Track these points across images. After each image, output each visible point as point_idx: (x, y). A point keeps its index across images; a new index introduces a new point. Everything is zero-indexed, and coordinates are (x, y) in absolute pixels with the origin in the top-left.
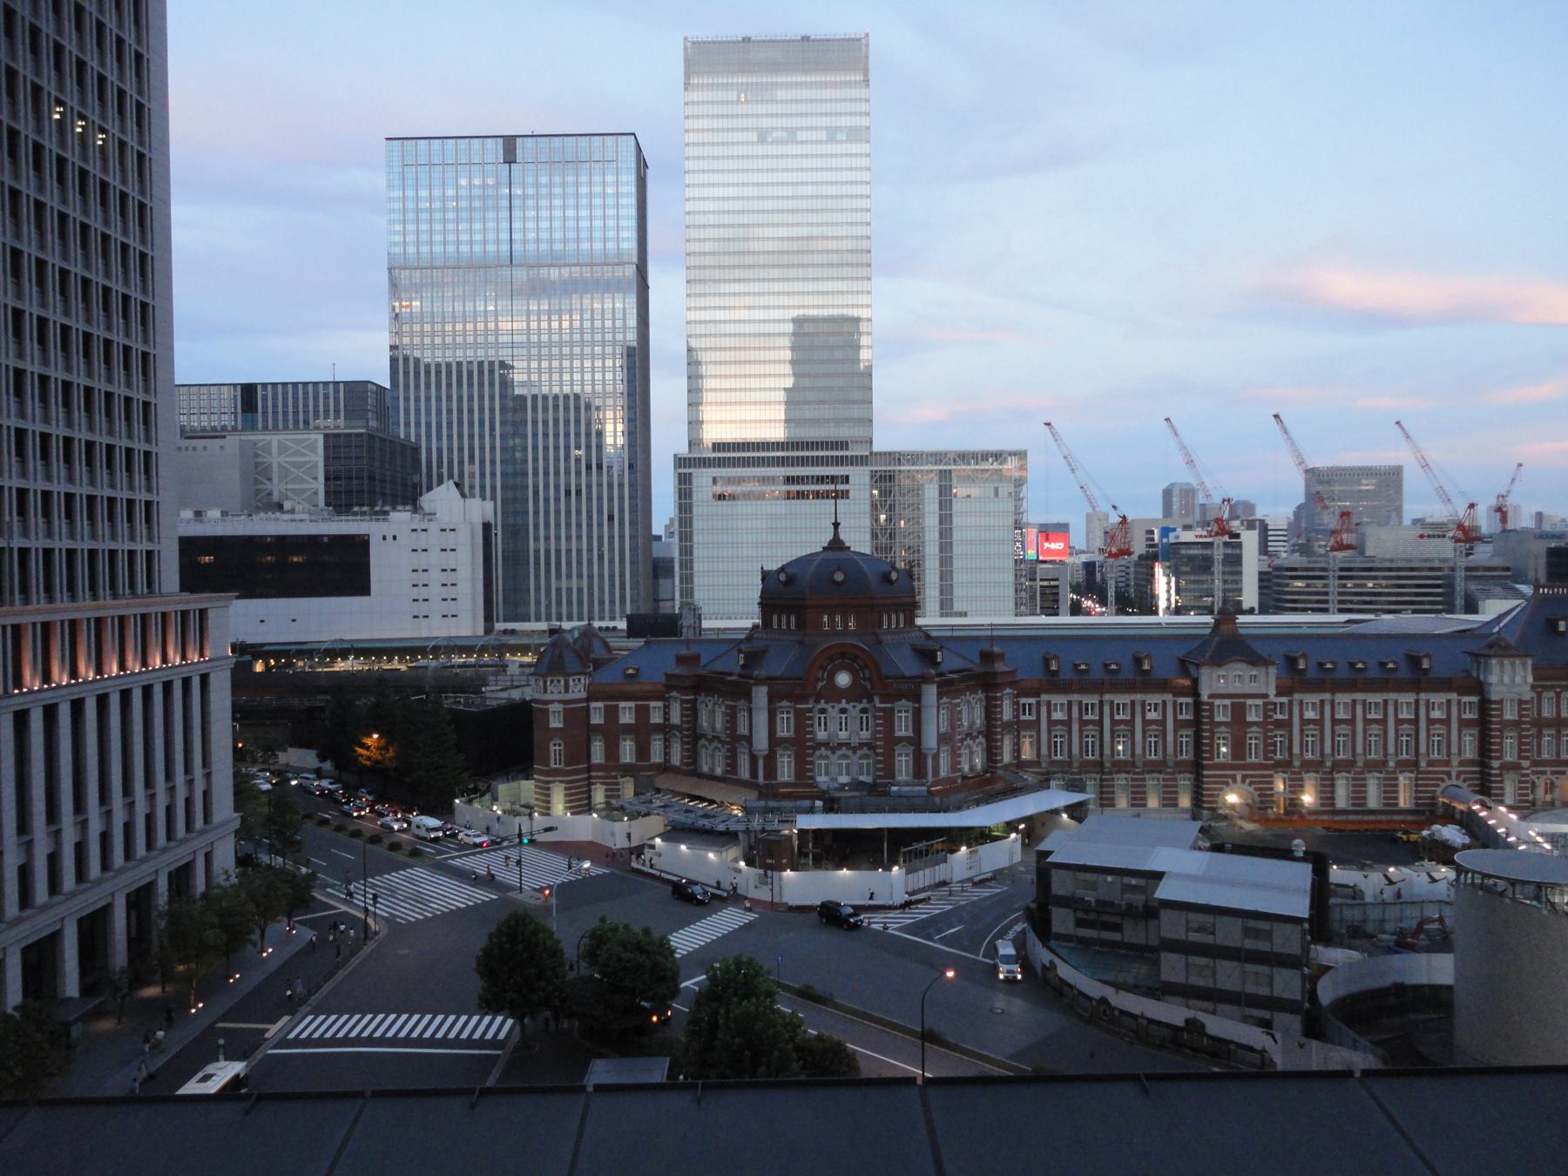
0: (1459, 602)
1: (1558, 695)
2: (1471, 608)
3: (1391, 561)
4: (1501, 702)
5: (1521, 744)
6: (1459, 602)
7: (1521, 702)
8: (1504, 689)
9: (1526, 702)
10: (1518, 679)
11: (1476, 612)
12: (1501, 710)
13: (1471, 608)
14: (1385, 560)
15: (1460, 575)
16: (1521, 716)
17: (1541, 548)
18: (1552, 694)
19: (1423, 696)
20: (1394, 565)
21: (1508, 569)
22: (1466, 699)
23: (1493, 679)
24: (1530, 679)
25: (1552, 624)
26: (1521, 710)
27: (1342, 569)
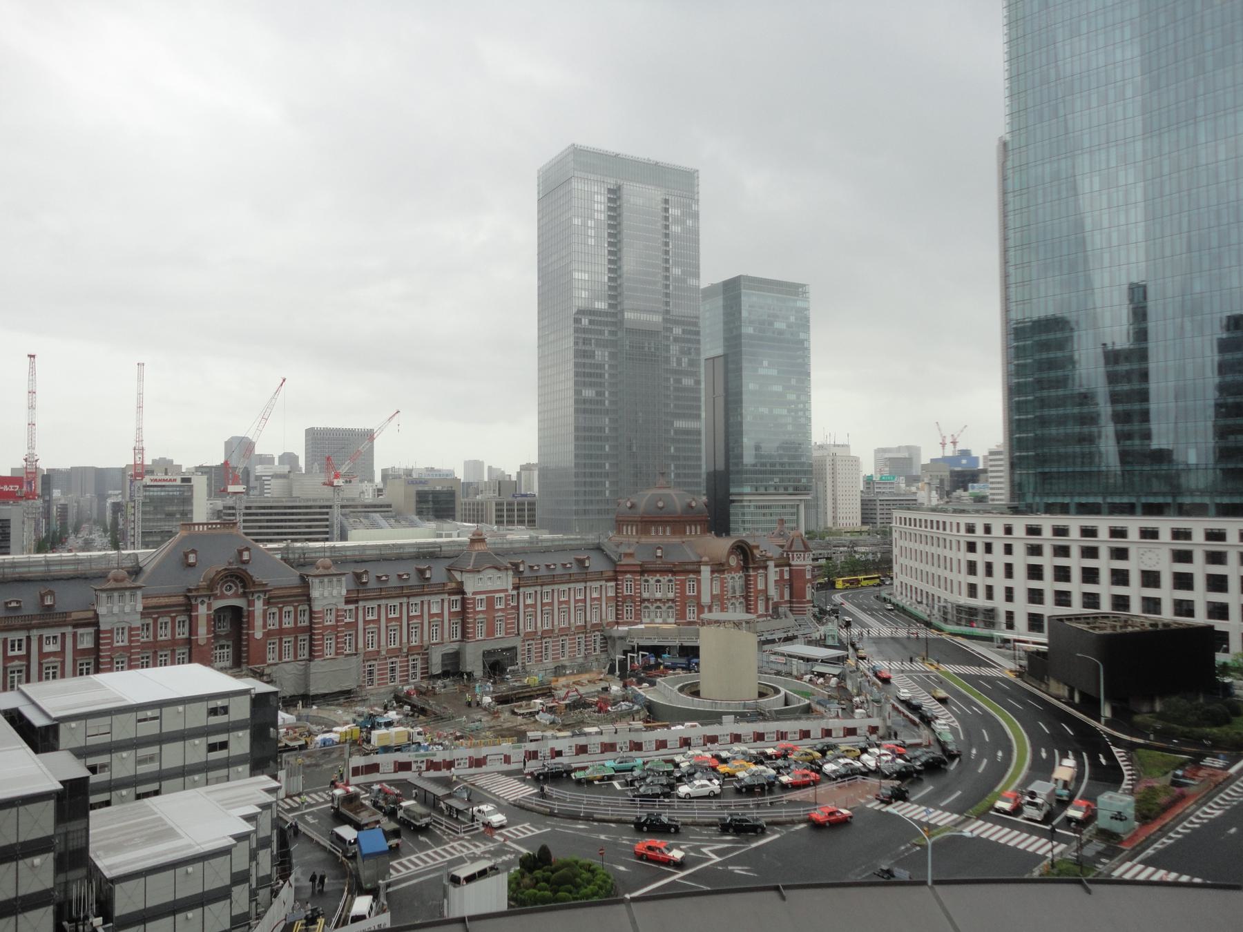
0: (336, 531)
1: (173, 619)
2: (343, 537)
3: (315, 500)
4: (111, 631)
5: (337, 643)
6: (336, 531)
7: (131, 629)
8: (115, 619)
9: (138, 629)
10: (127, 609)
11: (346, 539)
12: (111, 638)
13: (343, 537)
14: (308, 500)
15: (336, 512)
16: (130, 641)
17: (413, 490)
18: (167, 619)
19: (35, 633)
20: (309, 504)
21: (389, 506)
22: (80, 631)
23: (102, 610)
24: (140, 608)
25: (186, 556)
26: (130, 636)
27: (247, 508)
